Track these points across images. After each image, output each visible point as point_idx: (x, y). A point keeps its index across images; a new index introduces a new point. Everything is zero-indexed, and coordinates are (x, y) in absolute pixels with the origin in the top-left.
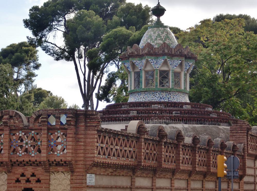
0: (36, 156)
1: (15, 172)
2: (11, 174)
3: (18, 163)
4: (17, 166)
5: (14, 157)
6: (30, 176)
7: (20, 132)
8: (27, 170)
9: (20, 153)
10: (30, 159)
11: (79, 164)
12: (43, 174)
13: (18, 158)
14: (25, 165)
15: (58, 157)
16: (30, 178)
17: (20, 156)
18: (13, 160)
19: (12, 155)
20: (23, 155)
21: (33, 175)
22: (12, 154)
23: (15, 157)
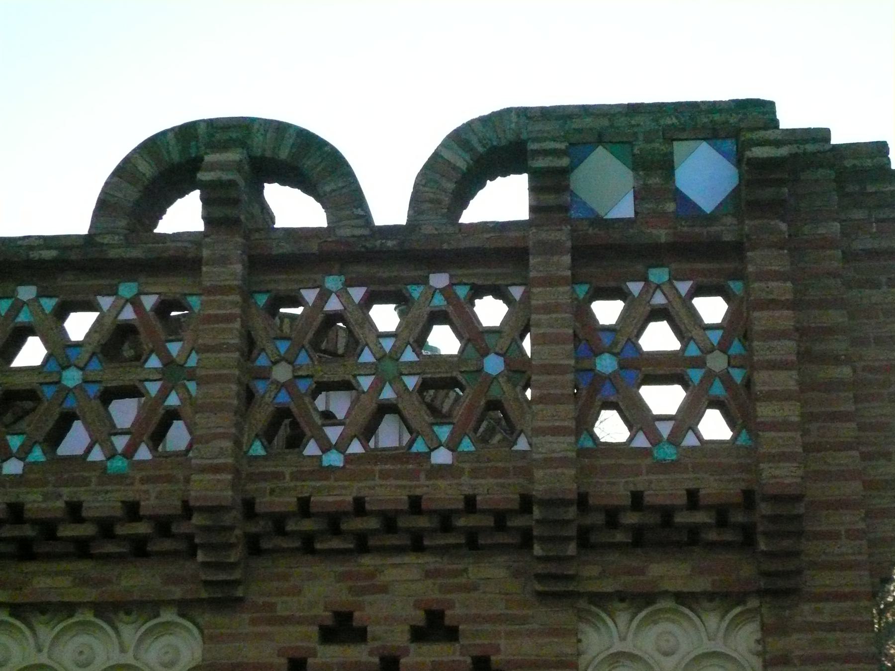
0: (466, 466)
1: (272, 607)
2: (240, 622)
3: (307, 525)
4: (292, 550)
5: (278, 476)
6: (407, 636)
7: (333, 282)
8: (384, 589)
9: (326, 447)
10: (418, 492)
11: (833, 536)
12: (524, 620)
13: (307, 487)
14: (363, 545)
15: (664, 467)
16: (406, 652)
17: (331, 469)
18: (265, 503)
19: (256, 457)
20: (350, 459)
21: (434, 627)
22: (258, 449)
23: (287, 471)
